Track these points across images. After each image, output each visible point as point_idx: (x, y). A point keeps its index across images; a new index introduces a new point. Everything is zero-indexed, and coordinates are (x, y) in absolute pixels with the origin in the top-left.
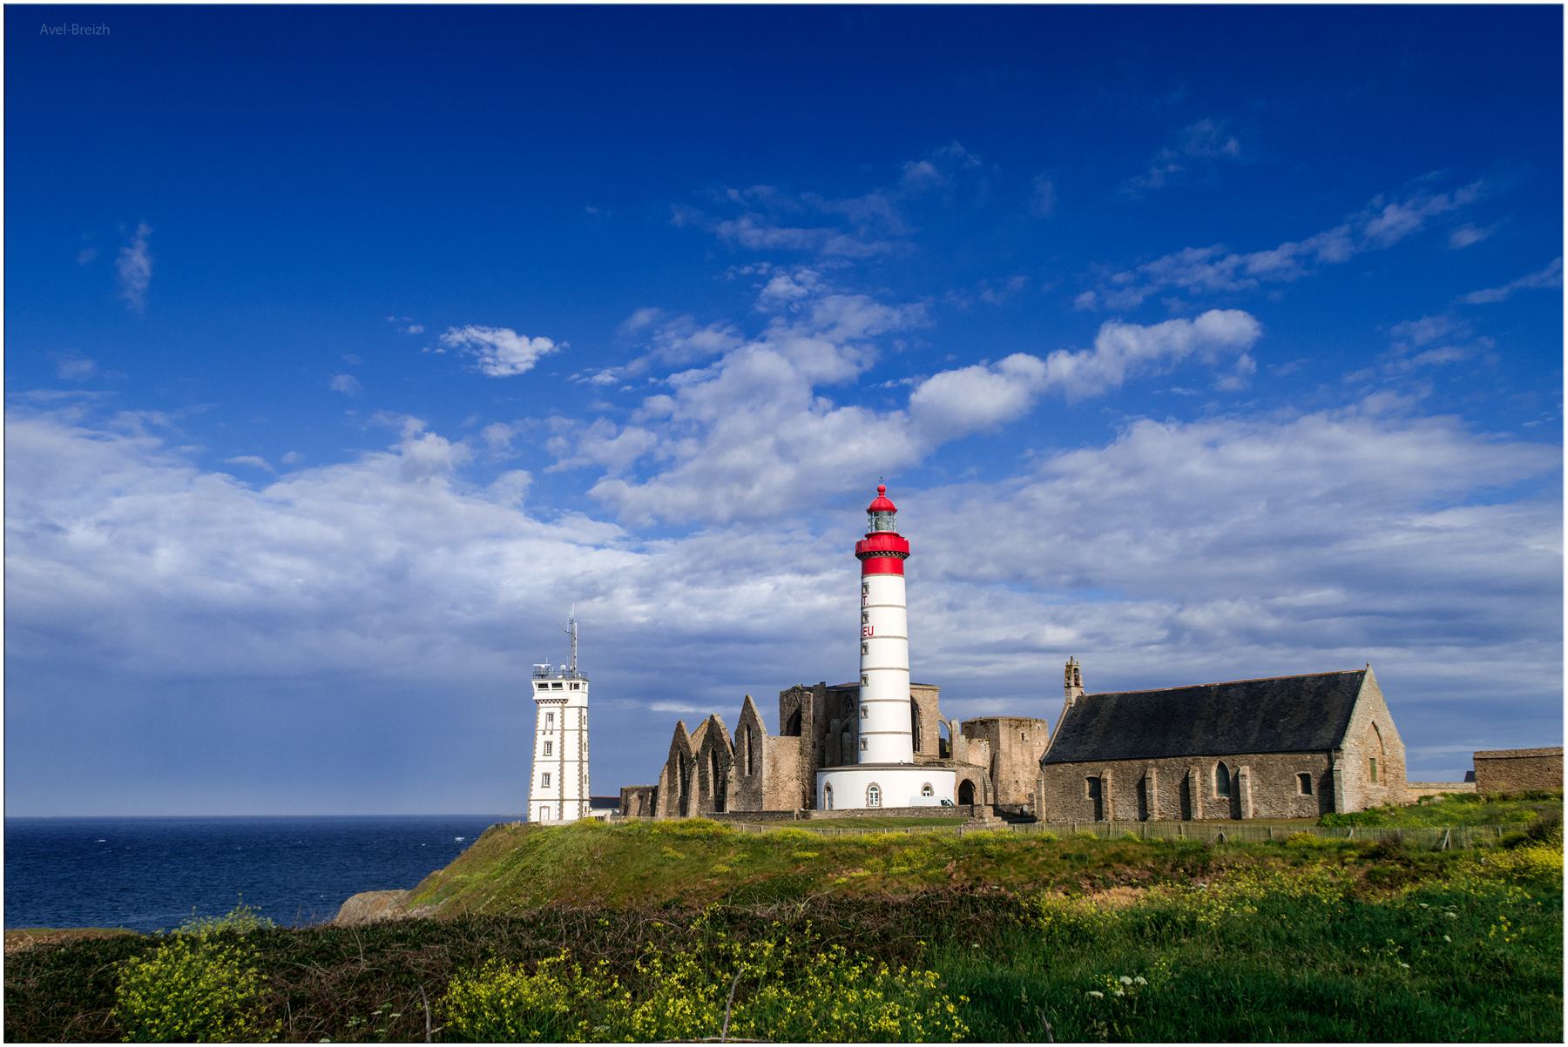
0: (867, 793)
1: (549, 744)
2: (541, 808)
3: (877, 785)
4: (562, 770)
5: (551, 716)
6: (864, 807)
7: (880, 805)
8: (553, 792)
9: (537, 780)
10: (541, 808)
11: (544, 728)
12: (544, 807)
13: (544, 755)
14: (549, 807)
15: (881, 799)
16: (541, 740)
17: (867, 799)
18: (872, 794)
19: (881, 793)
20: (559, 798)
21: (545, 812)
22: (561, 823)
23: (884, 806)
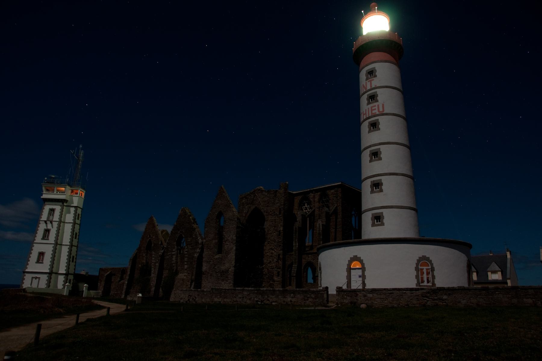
0: (417, 269)
1: (47, 231)
2: (33, 278)
3: (428, 259)
4: (54, 251)
5: (52, 211)
6: (412, 284)
7: (434, 284)
8: (45, 267)
9: (34, 256)
10: (33, 278)
11: (46, 220)
12: (36, 278)
13: (43, 238)
14: (39, 278)
15: (434, 277)
16: (42, 227)
17: (417, 277)
18: (422, 269)
19: (433, 269)
20: (48, 271)
21: (35, 282)
22: (49, 291)
23: (440, 283)
